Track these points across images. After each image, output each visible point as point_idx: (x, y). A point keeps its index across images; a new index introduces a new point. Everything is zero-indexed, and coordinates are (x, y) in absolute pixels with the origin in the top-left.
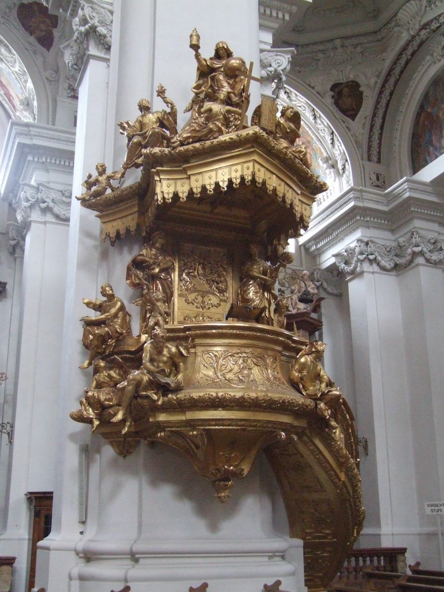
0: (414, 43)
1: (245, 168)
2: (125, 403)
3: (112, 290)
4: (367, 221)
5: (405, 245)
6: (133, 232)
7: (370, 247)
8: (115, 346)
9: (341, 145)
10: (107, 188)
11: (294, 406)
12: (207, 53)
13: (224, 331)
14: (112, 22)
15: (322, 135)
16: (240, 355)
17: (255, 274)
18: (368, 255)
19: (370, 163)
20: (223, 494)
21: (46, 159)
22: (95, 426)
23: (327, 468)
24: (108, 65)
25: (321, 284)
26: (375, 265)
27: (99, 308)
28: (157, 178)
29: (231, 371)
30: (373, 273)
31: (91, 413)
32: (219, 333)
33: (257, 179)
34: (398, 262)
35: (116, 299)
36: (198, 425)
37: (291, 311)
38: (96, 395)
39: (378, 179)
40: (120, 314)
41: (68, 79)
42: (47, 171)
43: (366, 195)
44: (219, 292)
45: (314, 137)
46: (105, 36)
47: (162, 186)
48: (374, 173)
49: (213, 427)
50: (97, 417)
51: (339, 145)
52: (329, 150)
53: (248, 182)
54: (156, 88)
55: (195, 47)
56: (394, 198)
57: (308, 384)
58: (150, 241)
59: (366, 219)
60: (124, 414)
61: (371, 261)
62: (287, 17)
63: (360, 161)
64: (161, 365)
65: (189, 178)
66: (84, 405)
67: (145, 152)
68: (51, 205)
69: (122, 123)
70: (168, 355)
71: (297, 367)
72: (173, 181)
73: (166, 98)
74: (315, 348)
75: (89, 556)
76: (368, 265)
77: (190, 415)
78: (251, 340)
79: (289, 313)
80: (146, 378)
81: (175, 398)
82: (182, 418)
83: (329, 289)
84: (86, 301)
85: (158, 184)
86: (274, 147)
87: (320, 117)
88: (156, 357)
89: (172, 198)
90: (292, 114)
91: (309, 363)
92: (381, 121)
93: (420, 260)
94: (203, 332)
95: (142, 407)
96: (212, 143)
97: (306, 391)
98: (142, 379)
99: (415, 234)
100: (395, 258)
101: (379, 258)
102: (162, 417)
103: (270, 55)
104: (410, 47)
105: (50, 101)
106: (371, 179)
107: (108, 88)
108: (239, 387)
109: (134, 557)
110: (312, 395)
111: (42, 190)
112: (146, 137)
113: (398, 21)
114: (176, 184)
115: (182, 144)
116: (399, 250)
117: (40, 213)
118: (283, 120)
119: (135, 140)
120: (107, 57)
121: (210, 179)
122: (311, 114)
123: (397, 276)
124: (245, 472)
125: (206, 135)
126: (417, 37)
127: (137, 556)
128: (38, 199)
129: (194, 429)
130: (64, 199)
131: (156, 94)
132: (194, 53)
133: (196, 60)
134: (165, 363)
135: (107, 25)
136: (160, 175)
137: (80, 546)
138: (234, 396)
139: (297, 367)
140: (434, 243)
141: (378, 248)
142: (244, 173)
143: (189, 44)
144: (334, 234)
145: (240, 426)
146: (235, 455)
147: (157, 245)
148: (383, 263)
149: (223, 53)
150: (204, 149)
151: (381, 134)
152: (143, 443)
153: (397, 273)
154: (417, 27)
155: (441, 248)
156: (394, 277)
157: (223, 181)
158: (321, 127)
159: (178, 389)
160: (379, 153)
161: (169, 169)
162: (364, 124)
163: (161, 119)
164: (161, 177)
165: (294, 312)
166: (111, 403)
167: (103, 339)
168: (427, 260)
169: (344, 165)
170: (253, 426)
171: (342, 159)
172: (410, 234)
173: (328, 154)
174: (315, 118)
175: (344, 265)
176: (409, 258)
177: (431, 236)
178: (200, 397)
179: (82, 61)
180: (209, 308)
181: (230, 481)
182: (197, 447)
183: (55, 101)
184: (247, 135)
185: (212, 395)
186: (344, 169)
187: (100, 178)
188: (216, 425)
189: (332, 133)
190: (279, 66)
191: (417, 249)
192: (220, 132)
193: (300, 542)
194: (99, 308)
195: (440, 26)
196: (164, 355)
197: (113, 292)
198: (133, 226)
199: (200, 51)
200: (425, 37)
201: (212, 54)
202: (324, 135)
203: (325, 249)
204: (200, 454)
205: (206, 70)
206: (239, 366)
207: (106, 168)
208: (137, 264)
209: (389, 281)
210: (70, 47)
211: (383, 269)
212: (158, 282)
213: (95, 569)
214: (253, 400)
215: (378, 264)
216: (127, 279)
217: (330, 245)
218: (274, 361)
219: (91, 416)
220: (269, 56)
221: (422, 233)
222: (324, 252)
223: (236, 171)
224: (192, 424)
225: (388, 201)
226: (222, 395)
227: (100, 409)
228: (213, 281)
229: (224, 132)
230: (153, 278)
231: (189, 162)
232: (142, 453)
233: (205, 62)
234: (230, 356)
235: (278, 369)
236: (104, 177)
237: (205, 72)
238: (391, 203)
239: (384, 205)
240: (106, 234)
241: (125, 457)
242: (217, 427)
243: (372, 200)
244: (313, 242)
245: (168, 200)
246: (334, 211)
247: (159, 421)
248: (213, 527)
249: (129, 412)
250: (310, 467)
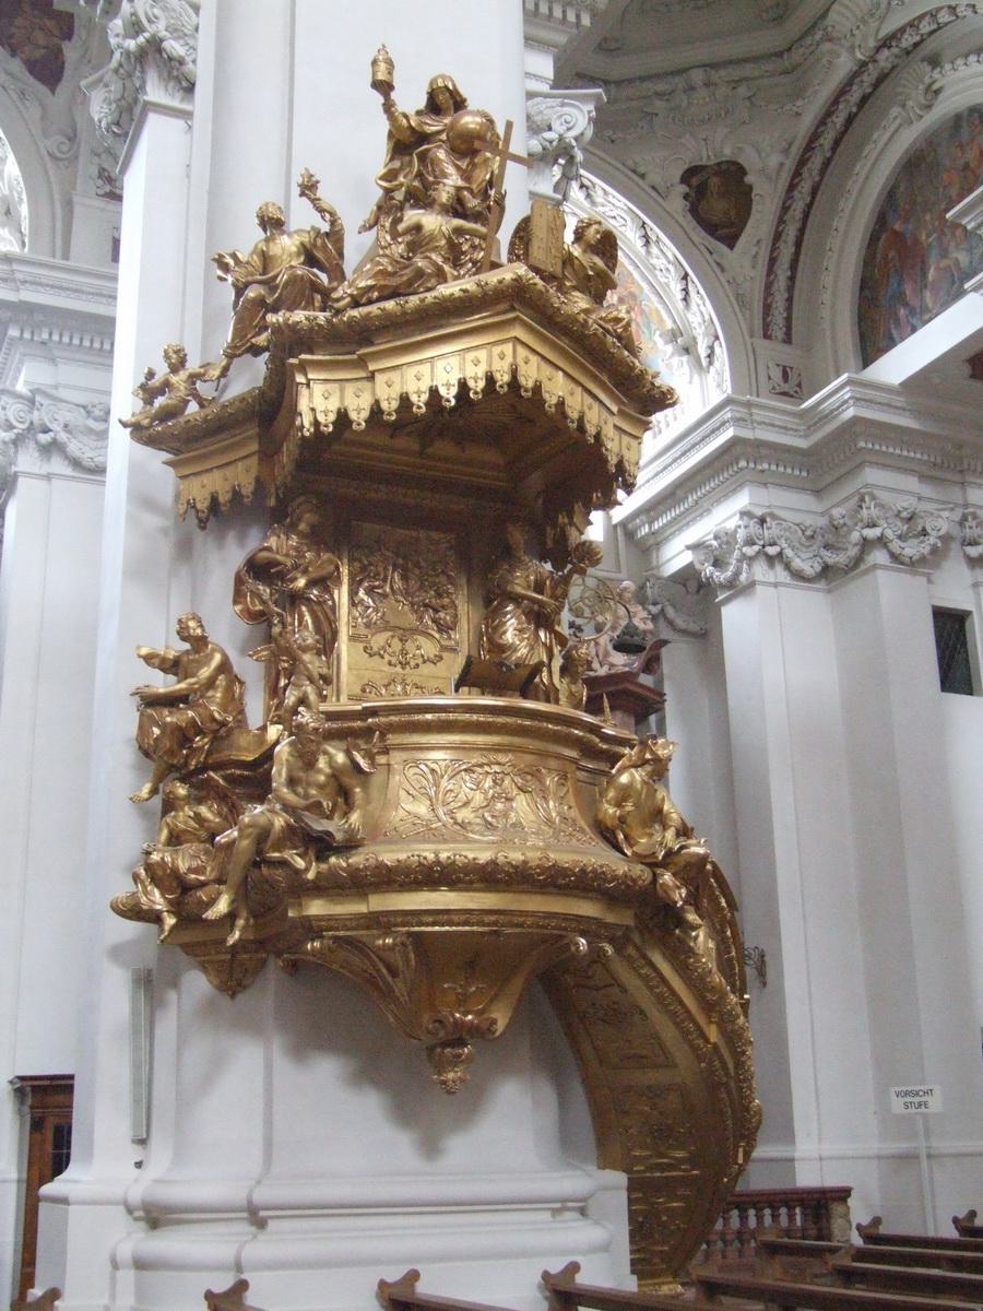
0: (865, 77)
1: (496, 358)
2: (235, 875)
3: (201, 626)
4: (762, 471)
5: (845, 524)
7: (768, 529)
8: (209, 753)
9: (704, 304)
10: (189, 401)
11: (605, 880)
12: (410, 100)
13: (451, 716)
14: (197, 29)
15: (663, 280)
16: (487, 768)
17: (519, 590)
18: (764, 546)
19: (766, 342)
20: (451, 1075)
21: (51, 334)
22: (167, 928)
23: (680, 1016)
24: (190, 127)
25: (663, 610)
26: (779, 568)
27: (173, 666)
28: (300, 378)
29: (466, 804)
30: (776, 585)
31: (157, 900)
32: (440, 720)
33: (522, 381)
34: (830, 561)
35: (210, 646)
36: (396, 925)
37: (596, 671)
38: (168, 859)
39: (785, 377)
40: (221, 680)
41: (98, 155)
42: (53, 360)
43: (759, 414)
44: (440, 631)
45: (644, 285)
46: (181, 62)
47: (311, 396)
48: (778, 365)
49: (429, 929)
50: (173, 909)
51: (701, 302)
52: (679, 314)
53: (501, 386)
54: (297, 179)
55: (384, 87)
56: (820, 419)
57: (635, 833)
58: (286, 517)
59: (759, 467)
60: (232, 902)
61: (771, 560)
62: (586, 21)
63: (747, 338)
64: (313, 792)
65: (371, 377)
66: (142, 882)
67: (274, 320)
68: (63, 437)
69: (221, 256)
70: (328, 770)
71: (611, 794)
72: (336, 385)
73: (319, 199)
74: (652, 752)
75: (155, 1217)
76: (765, 567)
77: (380, 902)
78: (511, 735)
79: (592, 674)
80: (279, 822)
81: (344, 865)
82: (360, 908)
83: (680, 622)
84: (144, 651)
85: (304, 391)
86: (559, 309)
87: (658, 241)
88: (301, 774)
89: (333, 423)
90: (598, 236)
91: (639, 786)
92: (793, 250)
93: (879, 556)
94: (405, 718)
95: (273, 885)
96: (423, 300)
97: (631, 846)
98: (272, 824)
99: (867, 498)
100: (824, 552)
101: (789, 552)
102: (316, 908)
103: (549, 105)
104: (855, 87)
105: (58, 206)
106: (769, 378)
107: (188, 176)
108: (486, 839)
109: (256, 1217)
110: (646, 857)
111: (42, 405)
112: (277, 287)
113: (830, 29)
114: (342, 391)
115: (356, 304)
116: (832, 537)
117: (37, 454)
118: (580, 250)
119: (251, 293)
120: (186, 106)
121: (419, 380)
122: (637, 235)
123: (829, 591)
124: (500, 1027)
125: (410, 283)
126: (870, 66)
127: (262, 1214)
128: (32, 423)
129: (386, 935)
130: (92, 423)
131: (296, 191)
132: (379, 99)
133: (385, 117)
134: (321, 787)
135: (186, 35)
136: (308, 369)
137: (136, 1195)
138: (474, 859)
139: (611, 794)
140: (910, 519)
141: (785, 530)
142: (494, 368)
143: (370, 80)
144: (690, 500)
145: (488, 925)
146: (477, 988)
147: (302, 526)
148: (797, 563)
149: (444, 100)
150: (404, 313)
151: (792, 279)
152: (274, 967)
153: (828, 584)
154: (872, 43)
155: (924, 529)
156: (821, 595)
157: (448, 385)
158: (660, 262)
159: (350, 845)
160: (788, 320)
161: (328, 358)
162: (755, 256)
163: (308, 246)
164: (310, 376)
165: (602, 671)
166: (202, 878)
167: (183, 736)
168: (894, 557)
169: (711, 348)
170: (517, 925)
171: (706, 334)
172: (854, 501)
173: (675, 322)
174: (647, 243)
175: (711, 568)
176: (853, 552)
177: (905, 503)
178: (398, 861)
179: (129, 117)
180: (417, 665)
181: (466, 1046)
182: (394, 973)
183: (68, 205)
184: (500, 282)
185: (425, 858)
186: (710, 356)
187: (174, 379)
188: (434, 924)
189: (685, 277)
190: (569, 129)
191: (872, 533)
192: (441, 277)
193: (620, 1178)
194: (173, 666)
195: (922, 41)
196: (320, 771)
197: (203, 631)
199: (394, 95)
200: (889, 66)
201: (422, 103)
202: (666, 280)
203: (668, 532)
204: (399, 987)
205: (406, 136)
206: (486, 793)
207: (185, 355)
208: (259, 569)
209: (810, 604)
210: (102, 84)
211: (798, 576)
212: (304, 608)
213: (168, 1244)
214: (516, 867)
215: (787, 567)
216: (235, 602)
217: (679, 524)
218: (563, 781)
219: (159, 907)
220: (547, 107)
221: (883, 496)
222: (667, 539)
223: (476, 363)
224: (381, 922)
225: (809, 428)
226: (449, 858)
227: (179, 891)
228: (426, 606)
229: (449, 276)
230: (295, 599)
231: (371, 344)
232: (270, 987)
233: (405, 121)
234: (465, 770)
235: (571, 799)
236: (183, 375)
237: (406, 143)
238: (815, 431)
239: (800, 436)
240: (188, 503)
241: (233, 996)
242: (437, 928)
243: (773, 425)
244: (644, 518)
245: (326, 426)
246: (689, 450)
247: (308, 916)
248: (430, 1147)
249: (243, 894)
250: (642, 1012)
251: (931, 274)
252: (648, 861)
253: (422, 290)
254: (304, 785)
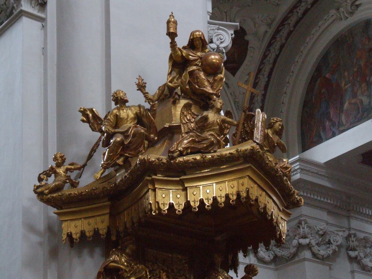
6: (103, 235)
12: (182, 41)
24: (43, 26)
28: (150, 187)
53: (243, 199)
55: (172, 35)
58: (119, 245)
73: (148, 93)
86: (267, 164)
96: (213, 157)
120: (42, 15)
125: (207, 147)
143: (166, 32)
147: (127, 251)
163: (139, 115)
164: (156, 186)
198: (103, 231)
199: (176, 39)
201: (186, 43)
207: (65, 159)
231: (185, 175)
253: (212, 151)
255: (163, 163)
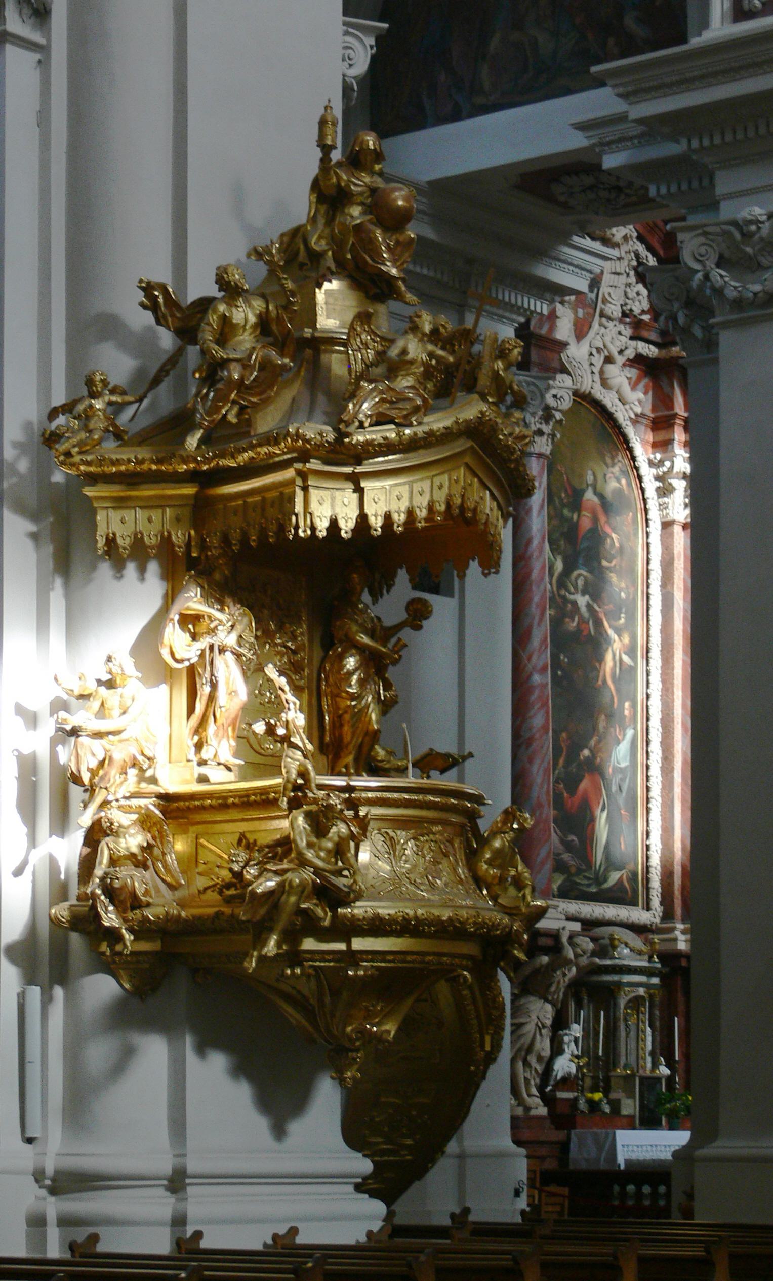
114: (333, 499)
120: (36, 37)
132: (319, 154)
134: (328, 851)
164: (310, 483)
178: (389, 915)
251: (494, 43)
252: (508, 911)
254: (317, 848)
255: (327, 441)
